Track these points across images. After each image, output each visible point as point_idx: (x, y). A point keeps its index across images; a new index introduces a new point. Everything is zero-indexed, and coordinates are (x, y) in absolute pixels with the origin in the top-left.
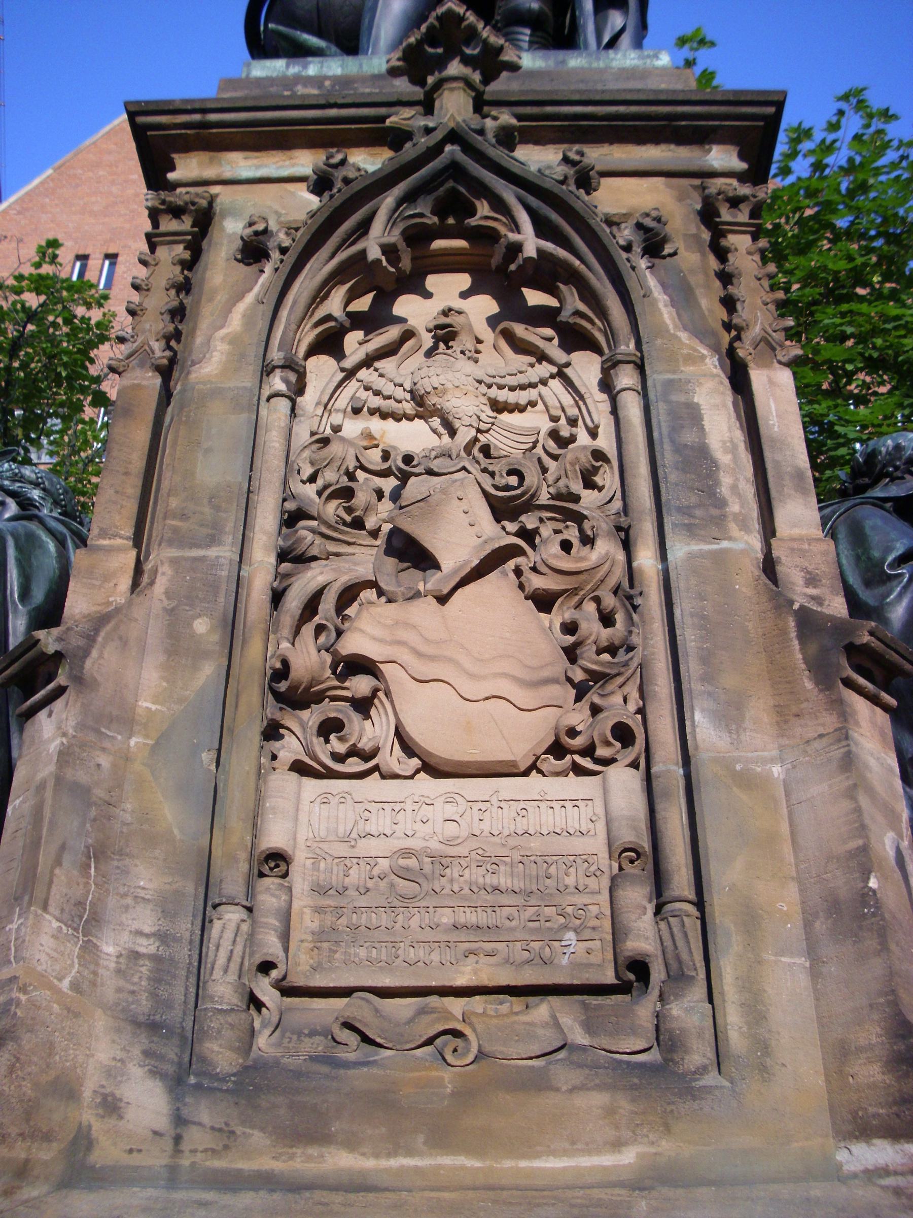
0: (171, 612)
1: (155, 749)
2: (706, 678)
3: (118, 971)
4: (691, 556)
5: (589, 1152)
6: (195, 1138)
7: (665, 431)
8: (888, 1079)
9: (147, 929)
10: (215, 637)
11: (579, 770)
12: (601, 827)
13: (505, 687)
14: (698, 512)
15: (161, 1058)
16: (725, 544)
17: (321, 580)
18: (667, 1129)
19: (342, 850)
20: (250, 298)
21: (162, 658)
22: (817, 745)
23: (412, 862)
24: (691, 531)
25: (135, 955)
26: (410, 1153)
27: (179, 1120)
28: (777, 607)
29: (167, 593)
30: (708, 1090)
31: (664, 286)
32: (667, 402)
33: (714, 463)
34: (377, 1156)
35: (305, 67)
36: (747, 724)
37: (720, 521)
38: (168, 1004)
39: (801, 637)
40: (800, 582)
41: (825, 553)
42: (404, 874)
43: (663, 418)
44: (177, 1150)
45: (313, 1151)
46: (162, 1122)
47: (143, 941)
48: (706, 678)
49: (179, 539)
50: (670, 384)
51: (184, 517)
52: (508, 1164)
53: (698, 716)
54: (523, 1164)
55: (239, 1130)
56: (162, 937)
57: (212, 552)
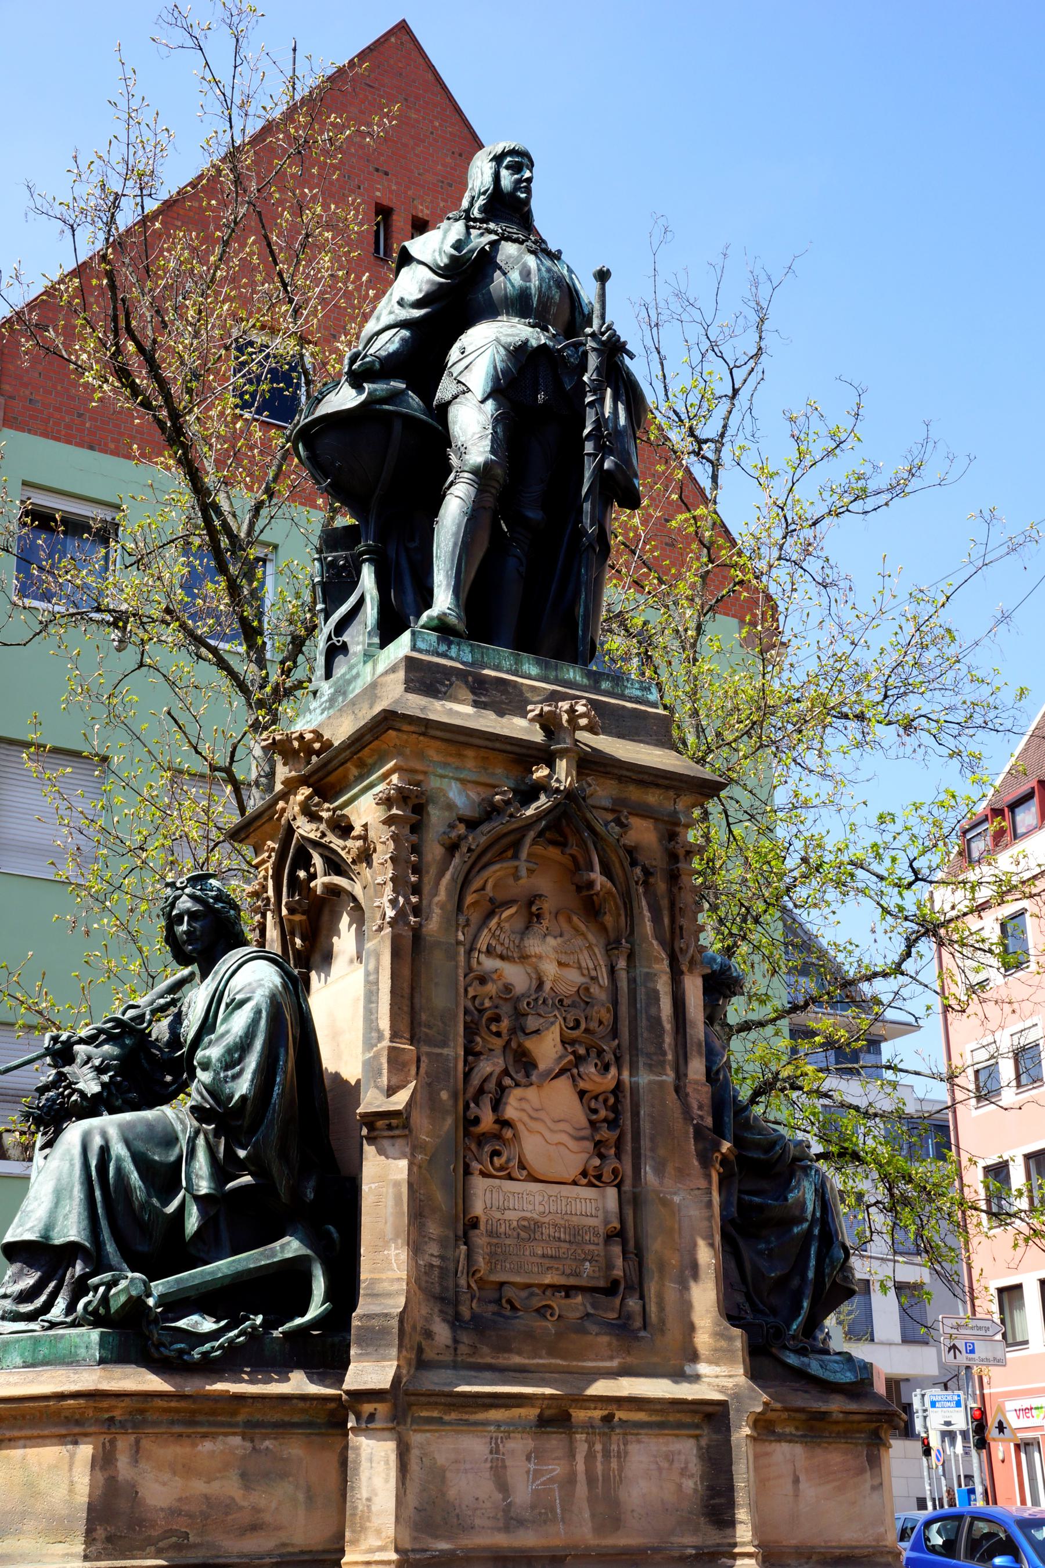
0: (429, 1085)
1: (430, 1161)
2: (652, 1150)
3: (425, 1273)
4: (650, 1082)
5: (602, 1360)
6: (463, 1349)
7: (643, 1005)
8: (711, 1341)
9: (436, 1254)
10: (451, 1103)
11: (590, 1184)
12: (600, 1214)
13: (564, 1138)
14: (655, 1058)
15: (446, 1313)
16: (664, 1078)
17: (489, 1070)
18: (629, 1353)
19: (498, 1215)
20: (448, 876)
21: (428, 1112)
22: (696, 1192)
23: (526, 1223)
24: (650, 1068)
25: (432, 1266)
26: (541, 1357)
27: (456, 1341)
28: (685, 1119)
29: (426, 1073)
30: (643, 1337)
31: (648, 904)
32: (646, 987)
33: (663, 1028)
34: (529, 1358)
35: (449, 648)
36: (666, 1175)
37: (662, 1064)
38: (446, 1289)
39: (696, 1138)
40: (696, 1107)
41: (707, 1093)
42: (524, 1228)
43: (643, 997)
44: (456, 1355)
45: (506, 1355)
46: (449, 1342)
47: (434, 1259)
48: (652, 1150)
49: (429, 1042)
50: (647, 974)
51: (429, 1027)
52: (575, 1363)
53: (648, 1168)
54: (580, 1364)
55: (478, 1346)
56: (442, 1257)
57: (445, 1051)
